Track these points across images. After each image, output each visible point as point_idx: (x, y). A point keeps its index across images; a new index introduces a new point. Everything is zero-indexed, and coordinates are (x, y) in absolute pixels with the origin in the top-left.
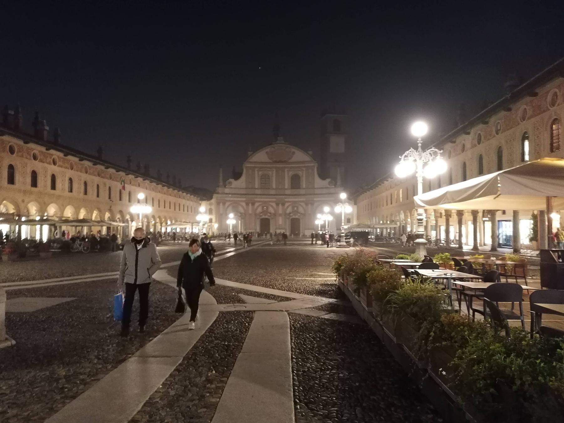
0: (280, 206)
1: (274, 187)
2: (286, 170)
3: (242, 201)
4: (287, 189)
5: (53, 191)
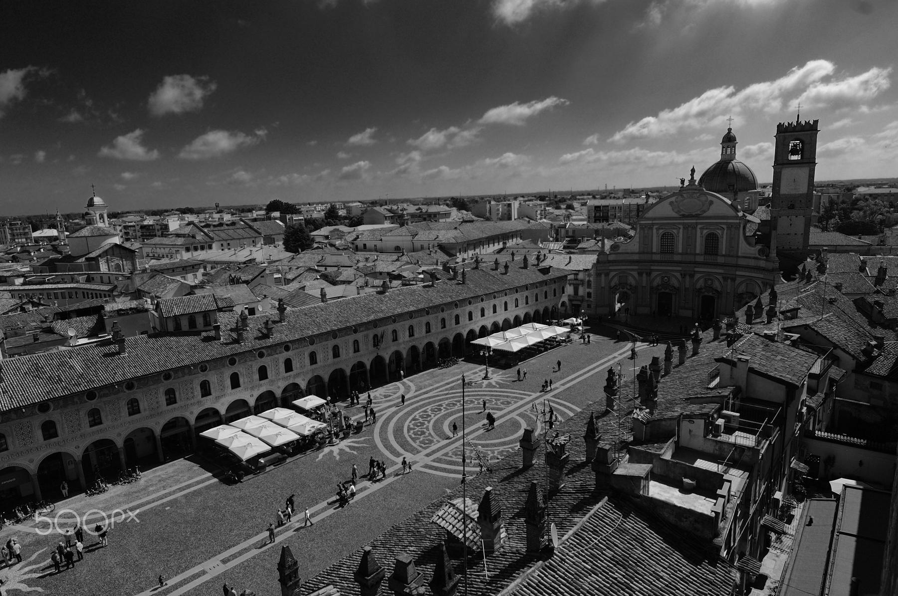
0: (688, 278)
1: (680, 251)
2: (699, 226)
3: (633, 270)
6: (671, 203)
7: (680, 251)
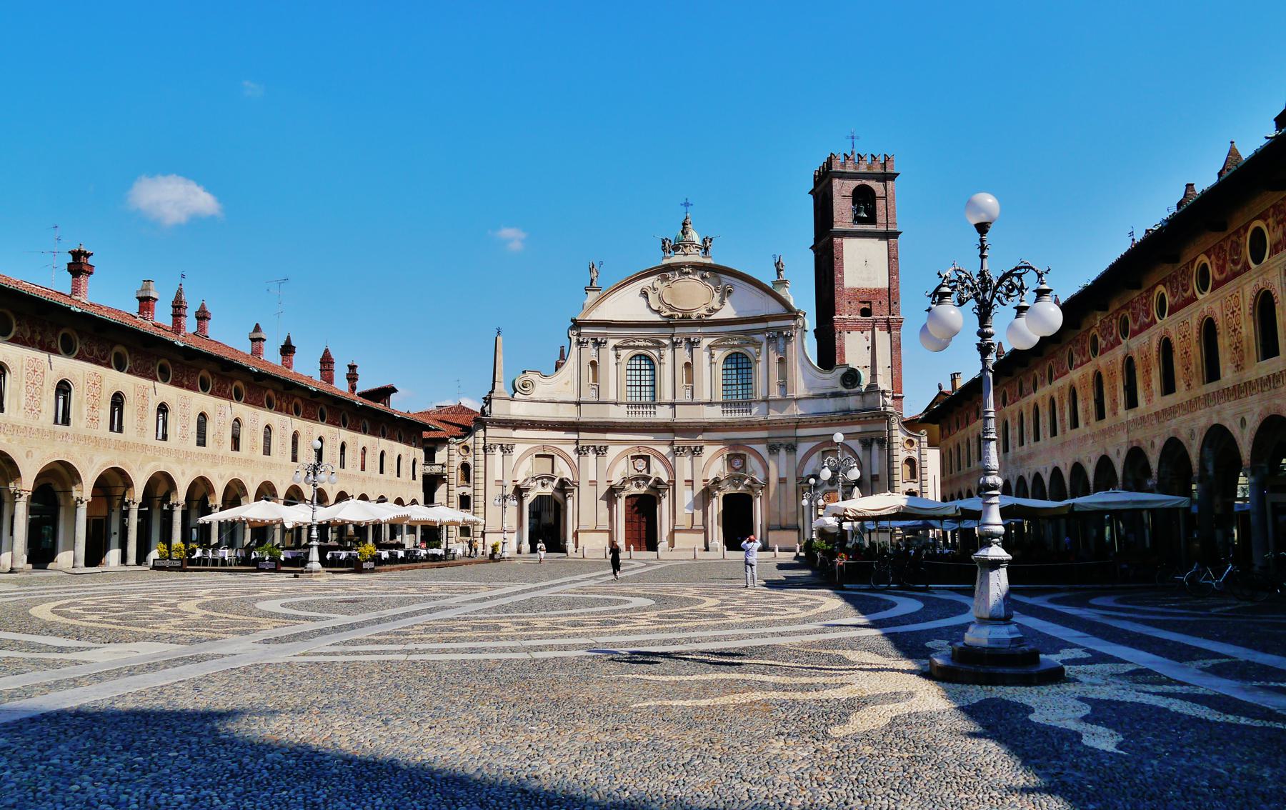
1: (668, 397)
4: (710, 404)
6: (644, 294)
7: (668, 397)
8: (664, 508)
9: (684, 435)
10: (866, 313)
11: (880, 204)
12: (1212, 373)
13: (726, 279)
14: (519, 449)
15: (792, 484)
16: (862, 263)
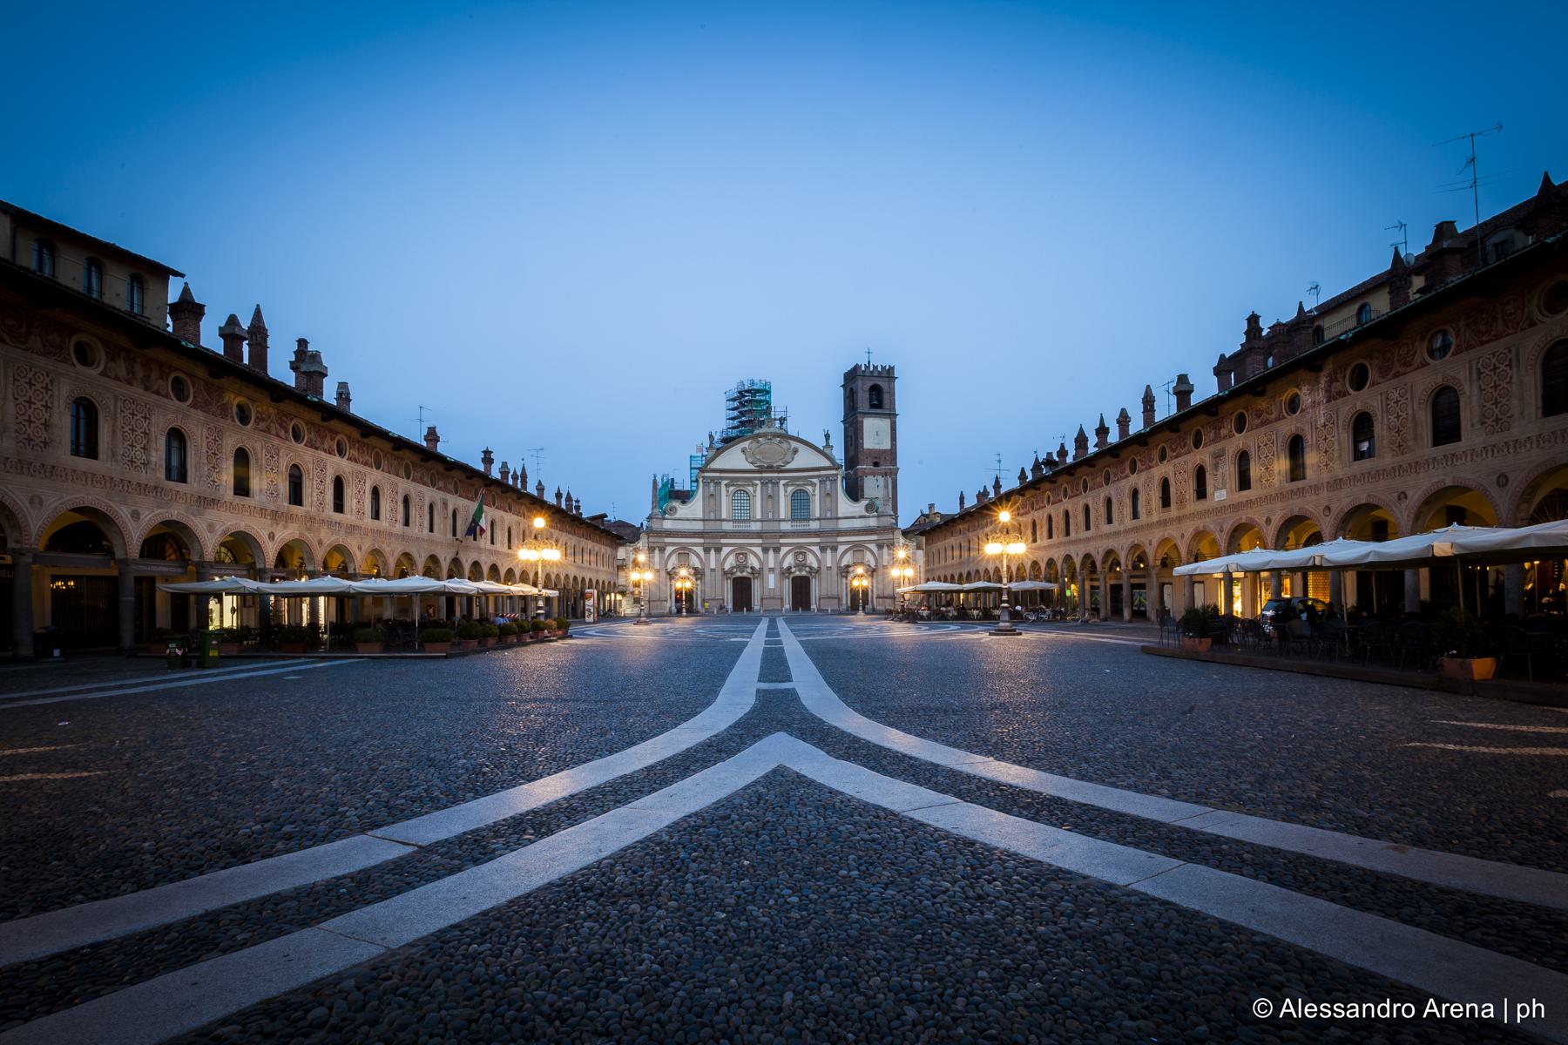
0: (771, 553)
1: (759, 516)
5: (337, 516)
6: (743, 451)
7: (759, 516)
8: (756, 586)
9: (771, 540)
10: (876, 464)
11: (886, 396)
12: (1068, 534)
13: (794, 444)
14: (669, 549)
15: (835, 570)
16: (874, 432)
